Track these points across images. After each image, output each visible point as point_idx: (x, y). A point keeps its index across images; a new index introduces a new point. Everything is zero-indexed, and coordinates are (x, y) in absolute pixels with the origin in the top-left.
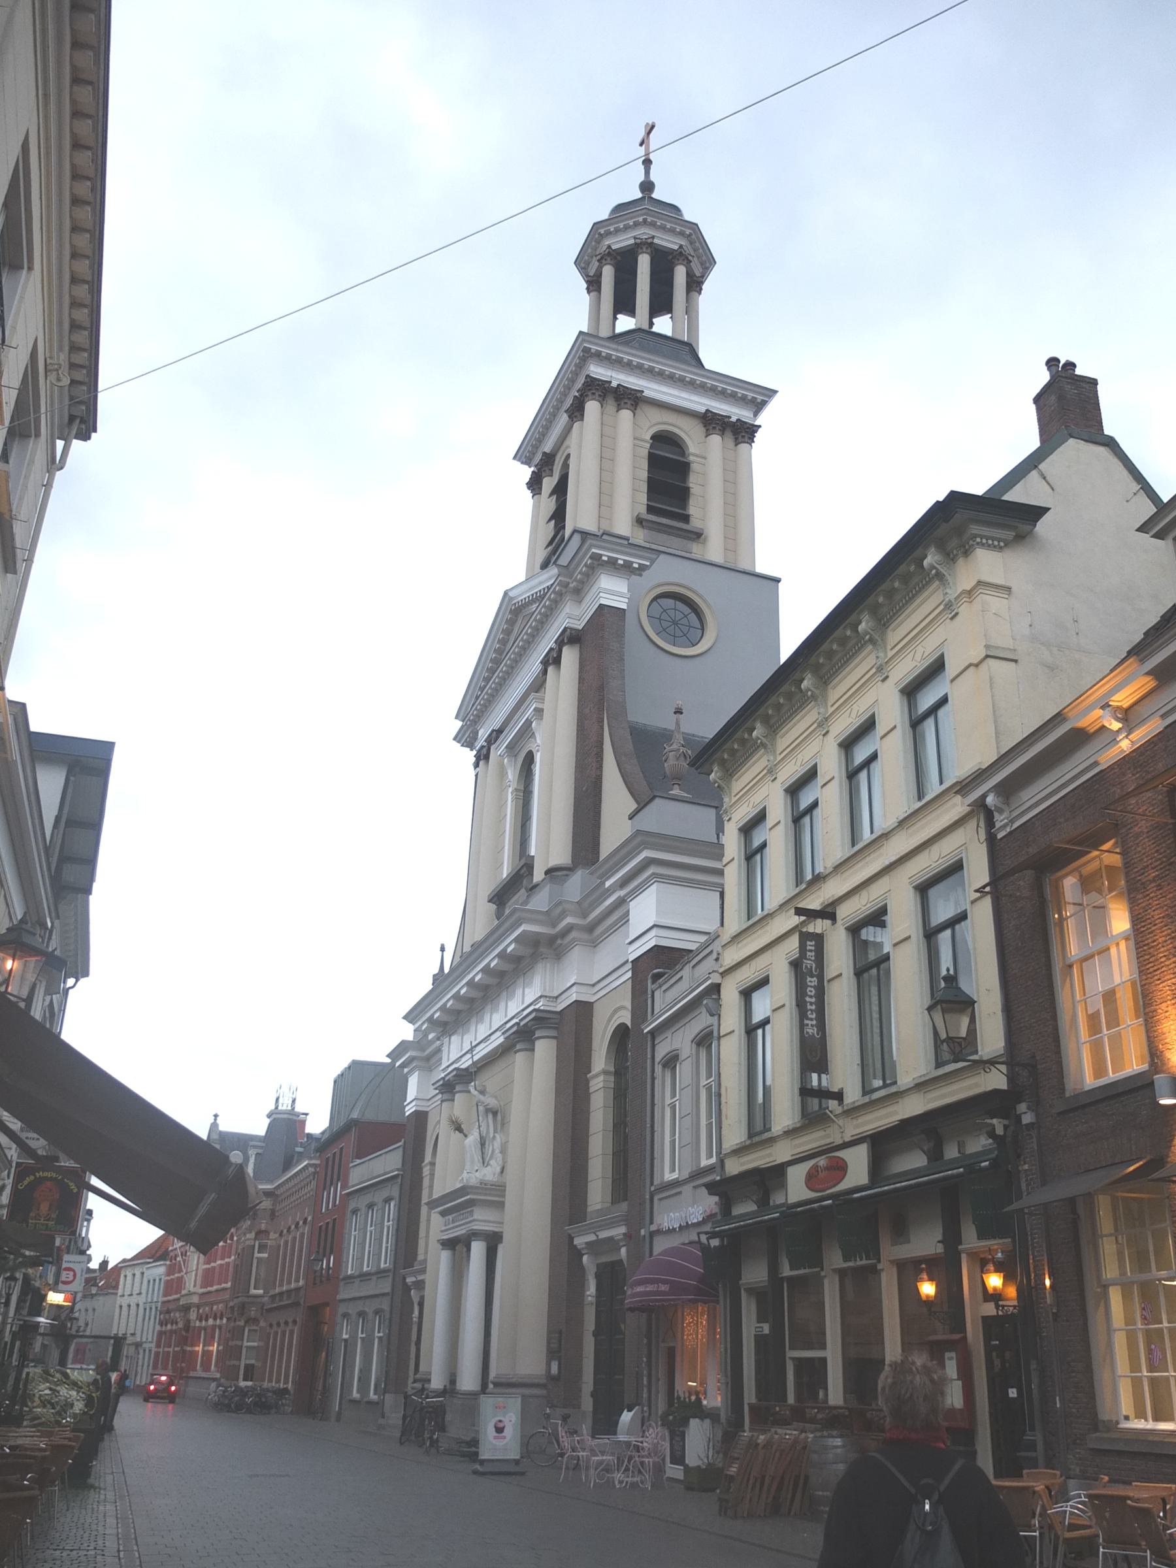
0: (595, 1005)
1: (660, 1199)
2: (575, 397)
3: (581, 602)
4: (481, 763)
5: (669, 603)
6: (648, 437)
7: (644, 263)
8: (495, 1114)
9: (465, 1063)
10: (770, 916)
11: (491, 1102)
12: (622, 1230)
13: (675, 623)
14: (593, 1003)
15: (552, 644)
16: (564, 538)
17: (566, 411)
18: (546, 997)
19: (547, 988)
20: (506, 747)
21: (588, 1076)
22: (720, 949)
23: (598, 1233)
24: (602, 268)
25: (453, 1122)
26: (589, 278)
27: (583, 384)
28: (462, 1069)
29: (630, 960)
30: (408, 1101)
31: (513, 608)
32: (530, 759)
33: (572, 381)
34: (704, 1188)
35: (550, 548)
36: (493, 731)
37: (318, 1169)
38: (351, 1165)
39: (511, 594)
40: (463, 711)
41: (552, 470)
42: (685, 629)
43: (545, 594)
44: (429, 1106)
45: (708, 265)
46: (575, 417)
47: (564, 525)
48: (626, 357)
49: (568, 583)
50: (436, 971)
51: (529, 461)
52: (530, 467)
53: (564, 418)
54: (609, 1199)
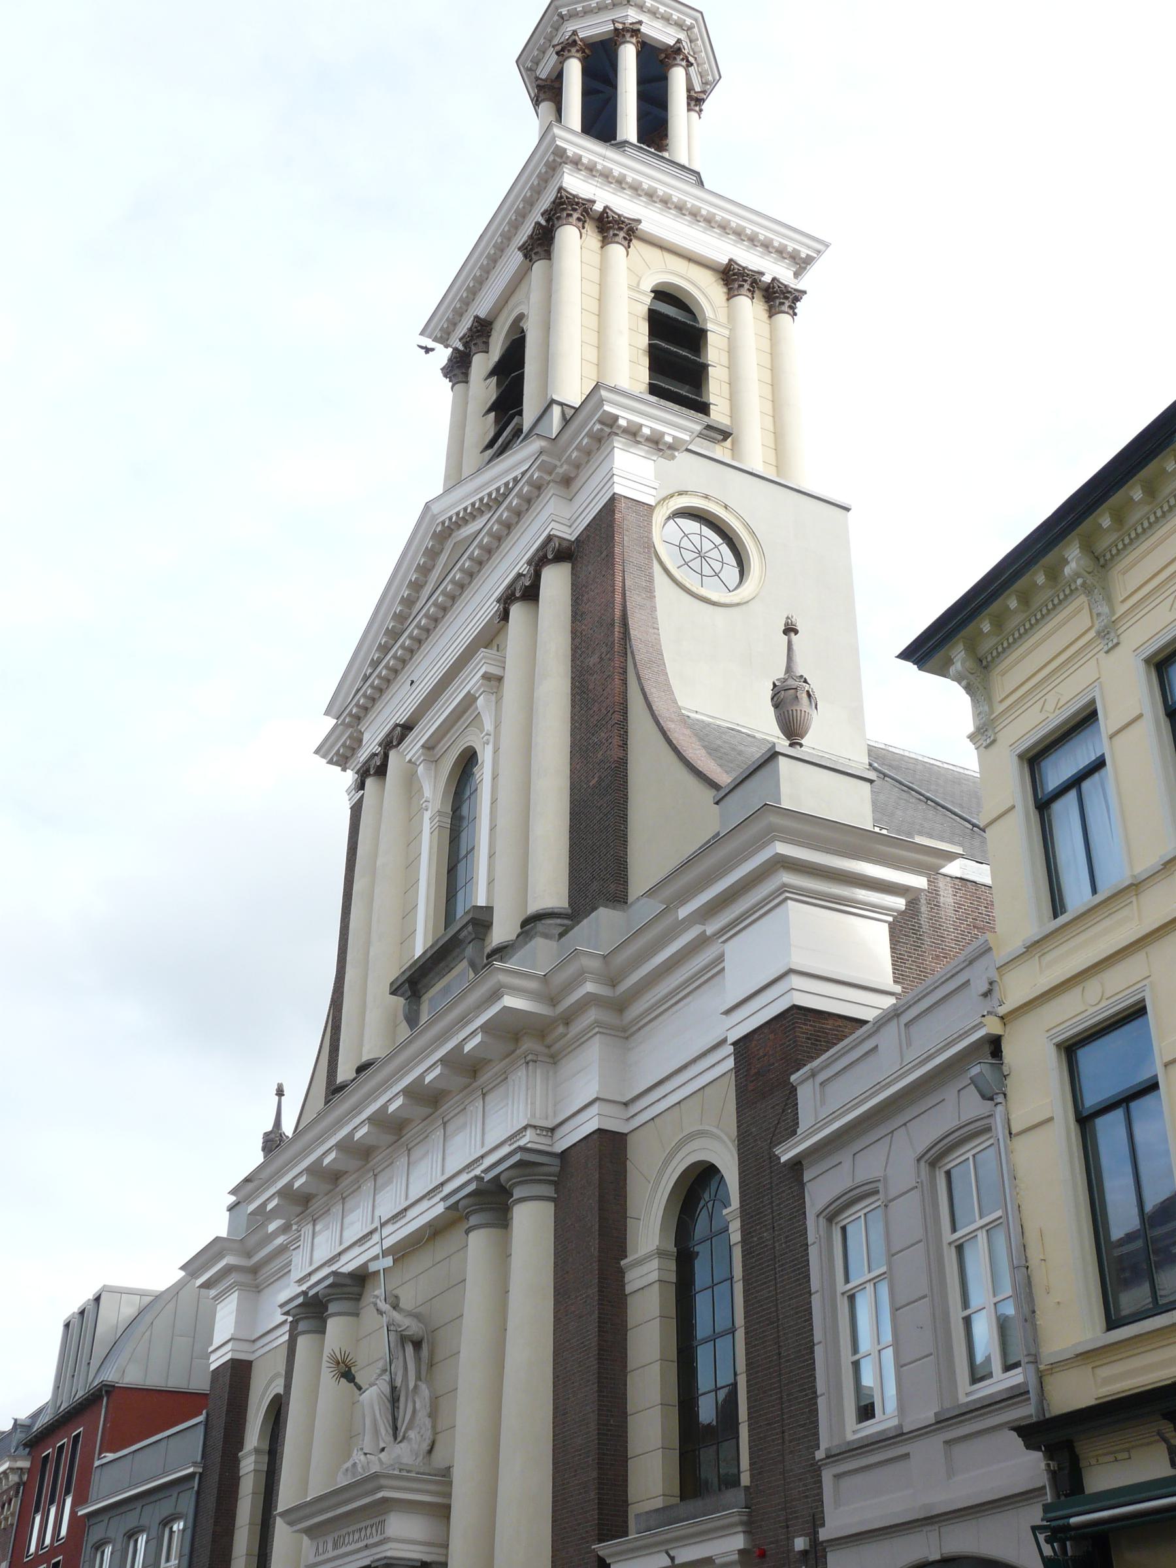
0: (629, 1137)
1: (838, 1477)
2: (538, 223)
3: (571, 500)
4: (369, 782)
7: (628, 56)
8: (417, 1345)
9: (348, 1264)
10: (1135, 887)
11: (413, 1327)
12: (738, 1542)
13: (701, 555)
14: (626, 1135)
15: (522, 567)
16: (520, 431)
17: (519, 249)
18: (535, 1127)
19: (538, 1115)
20: (423, 746)
21: (622, 1263)
22: (994, 975)
23: (672, 1553)
24: (562, 63)
25: (338, 1363)
26: (539, 82)
27: (554, 202)
29: (730, 1040)
30: (217, 1342)
31: (439, 528)
32: (468, 761)
33: (530, 203)
34: (1014, 1434)
35: (490, 452)
36: (397, 725)
37: (25, 1478)
38: (97, 1463)
39: (435, 509)
40: (340, 699)
41: (487, 343)
42: (717, 566)
43: (505, 496)
44: (253, 1352)
45: (710, 78)
46: (536, 253)
47: (522, 410)
48: (617, 171)
49: (556, 466)
50: (269, 1128)
51: (445, 336)
52: (447, 346)
53: (514, 259)
54: (677, 1491)
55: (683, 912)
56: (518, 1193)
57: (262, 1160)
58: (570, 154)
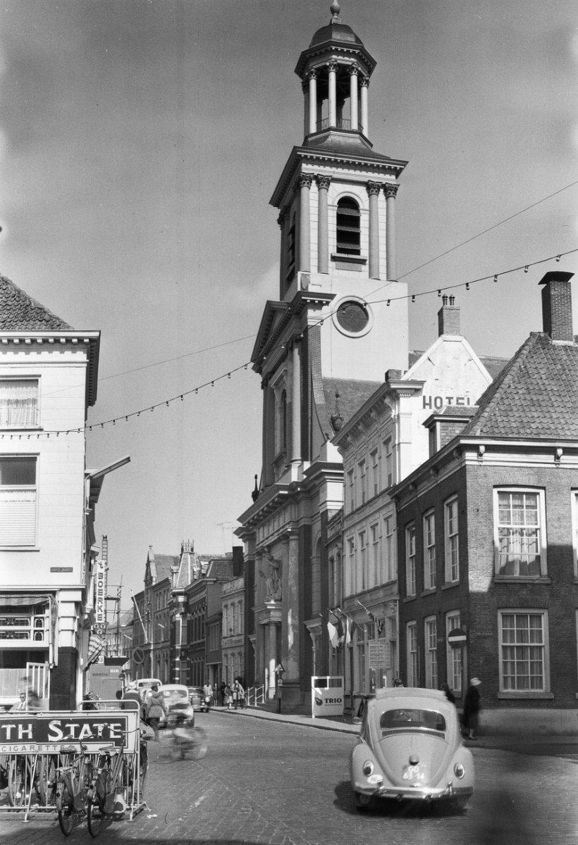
5: (350, 308)
6: (336, 204)
8: (277, 569)
57: (253, 503)
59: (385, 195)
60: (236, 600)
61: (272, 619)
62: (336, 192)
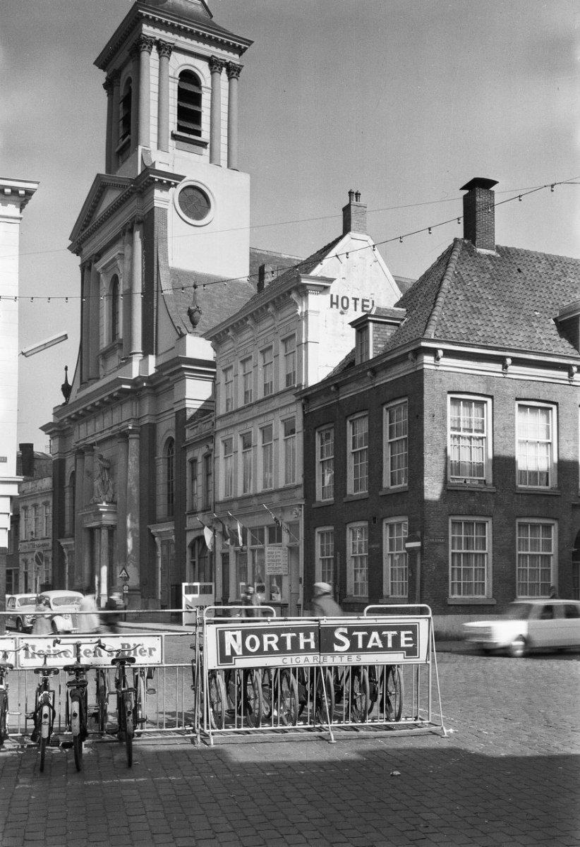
5: (191, 192)
6: (177, 76)
8: (108, 469)
11: (106, 465)
28: (88, 445)
55: (164, 374)
56: (130, 436)
58: (144, 15)
59: (228, 75)
60: (40, 501)
61: (104, 522)
62: (178, 63)
